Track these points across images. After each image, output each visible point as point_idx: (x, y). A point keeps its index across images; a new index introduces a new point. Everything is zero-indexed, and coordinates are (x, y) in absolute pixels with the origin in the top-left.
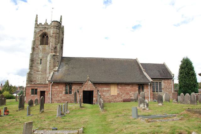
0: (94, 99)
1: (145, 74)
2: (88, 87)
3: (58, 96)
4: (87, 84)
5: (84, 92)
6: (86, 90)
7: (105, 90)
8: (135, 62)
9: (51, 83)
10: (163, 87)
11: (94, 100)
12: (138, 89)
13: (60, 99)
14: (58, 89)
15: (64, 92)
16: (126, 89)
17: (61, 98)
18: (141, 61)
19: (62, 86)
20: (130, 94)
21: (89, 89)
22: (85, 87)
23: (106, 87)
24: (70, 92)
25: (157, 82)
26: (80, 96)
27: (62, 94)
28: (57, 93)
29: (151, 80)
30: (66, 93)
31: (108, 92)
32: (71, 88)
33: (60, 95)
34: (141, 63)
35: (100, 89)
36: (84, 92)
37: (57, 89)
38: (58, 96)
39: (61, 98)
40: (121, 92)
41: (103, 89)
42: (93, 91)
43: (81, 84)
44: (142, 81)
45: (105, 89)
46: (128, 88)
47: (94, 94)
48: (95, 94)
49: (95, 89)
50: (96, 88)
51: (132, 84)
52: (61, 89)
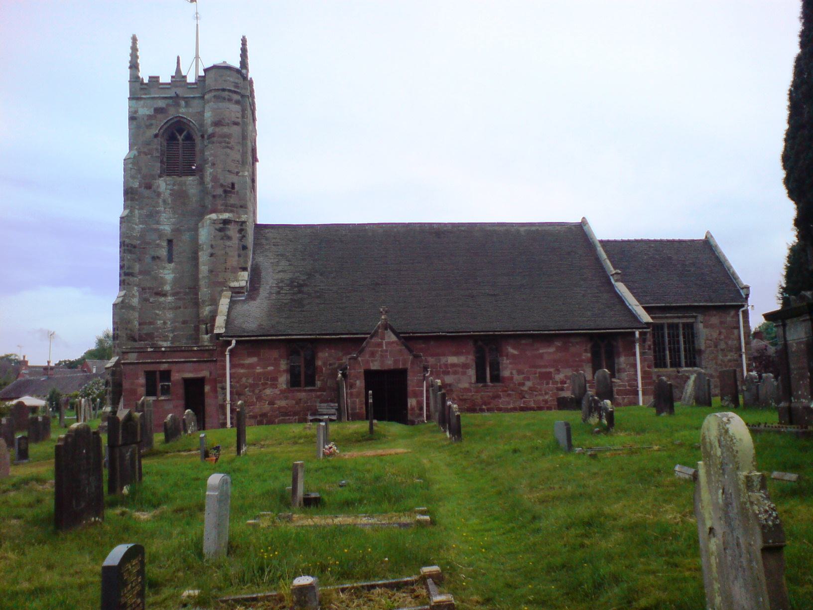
0: (412, 402)
1: (621, 288)
2: (386, 354)
3: (259, 398)
4: (380, 345)
5: (370, 375)
6: (375, 366)
7: (453, 365)
8: (578, 233)
9: (229, 343)
10: (702, 343)
11: (413, 409)
12: (589, 355)
13: (266, 407)
14: (259, 370)
15: (283, 380)
16: (541, 356)
17: (271, 403)
18: (603, 230)
19: (275, 354)
20: (559, 377)
21: (390, 363)
22: (373, 354)
23: (456, 354)
24: (311, 381)
25: (676, 321)
26: (356, 392)
27: (274, 386)
28: (253, 386)
29: (646, 318)
30: (295, 382)
31: (464, 373)
32: (310, 362)
33: (268, 391)
34: (605, 238)
35: (431, 360)
36: (370, 375)
37: (252, 366)
38: (259, 398)
39: (271, 403)
40: (520, 372)
41: (443, 360)
42: (403, 373)
43: (354, 343)
44: (610, 322)
45: (452, 360)
46: (548, 351)
47: (409, 382)
48: (412, 380)
49: (412, 363)
50: (416, 357)
51: (564, 337)
52: (270, 368)
